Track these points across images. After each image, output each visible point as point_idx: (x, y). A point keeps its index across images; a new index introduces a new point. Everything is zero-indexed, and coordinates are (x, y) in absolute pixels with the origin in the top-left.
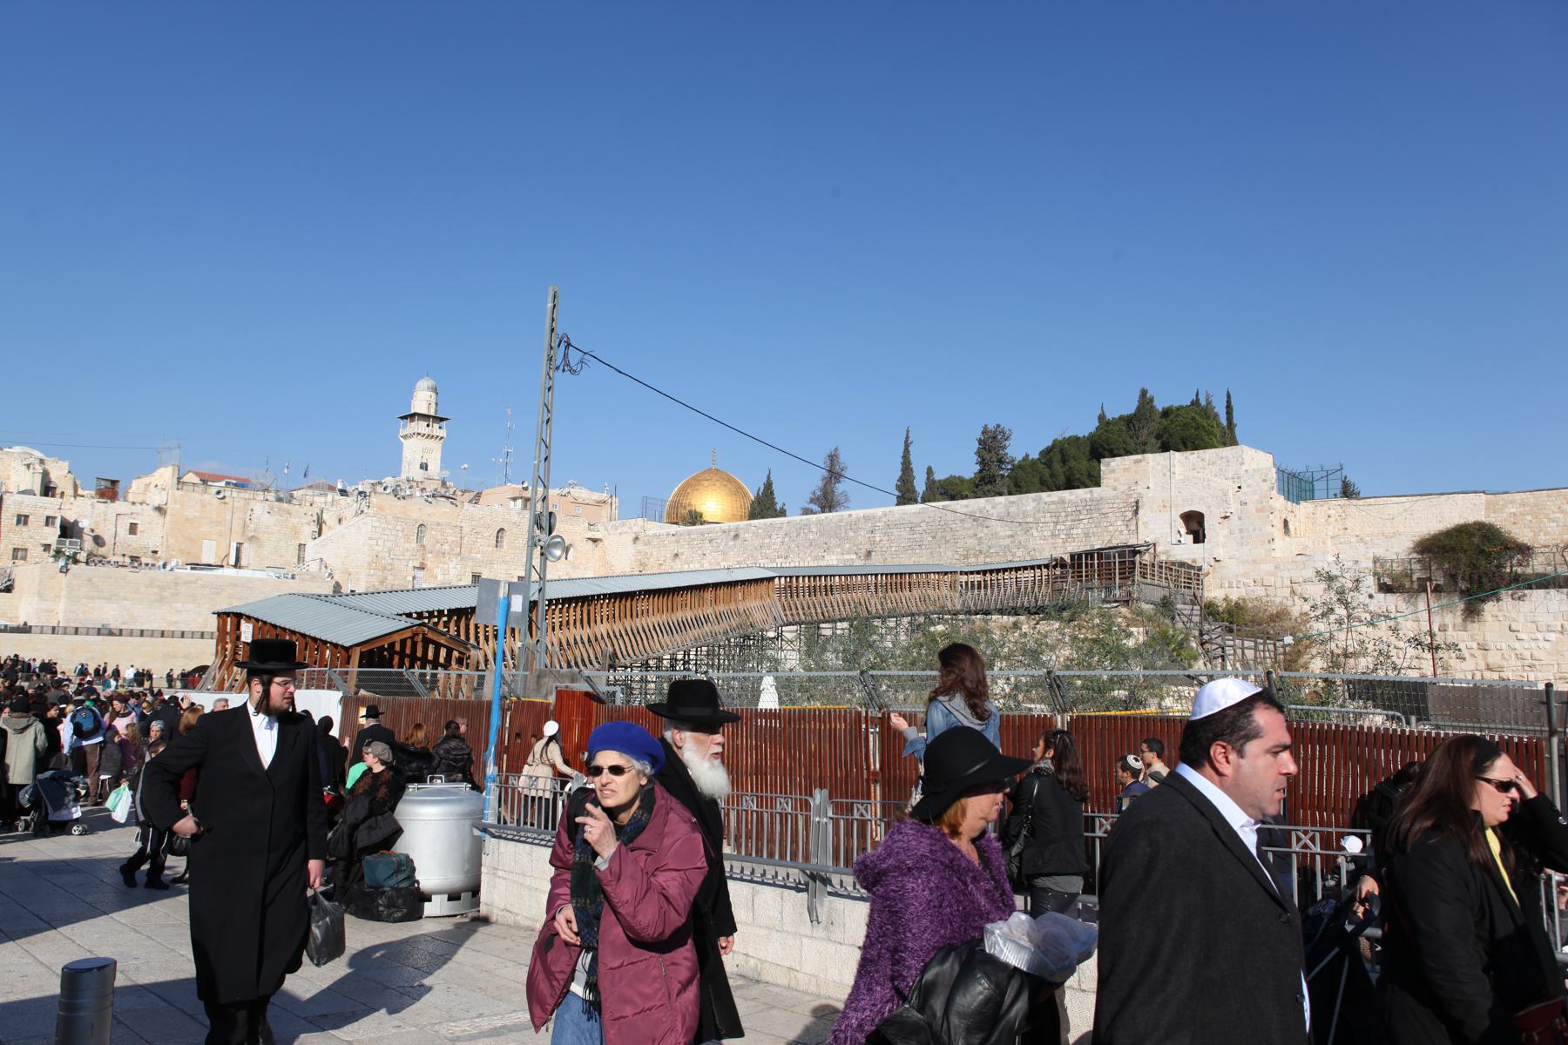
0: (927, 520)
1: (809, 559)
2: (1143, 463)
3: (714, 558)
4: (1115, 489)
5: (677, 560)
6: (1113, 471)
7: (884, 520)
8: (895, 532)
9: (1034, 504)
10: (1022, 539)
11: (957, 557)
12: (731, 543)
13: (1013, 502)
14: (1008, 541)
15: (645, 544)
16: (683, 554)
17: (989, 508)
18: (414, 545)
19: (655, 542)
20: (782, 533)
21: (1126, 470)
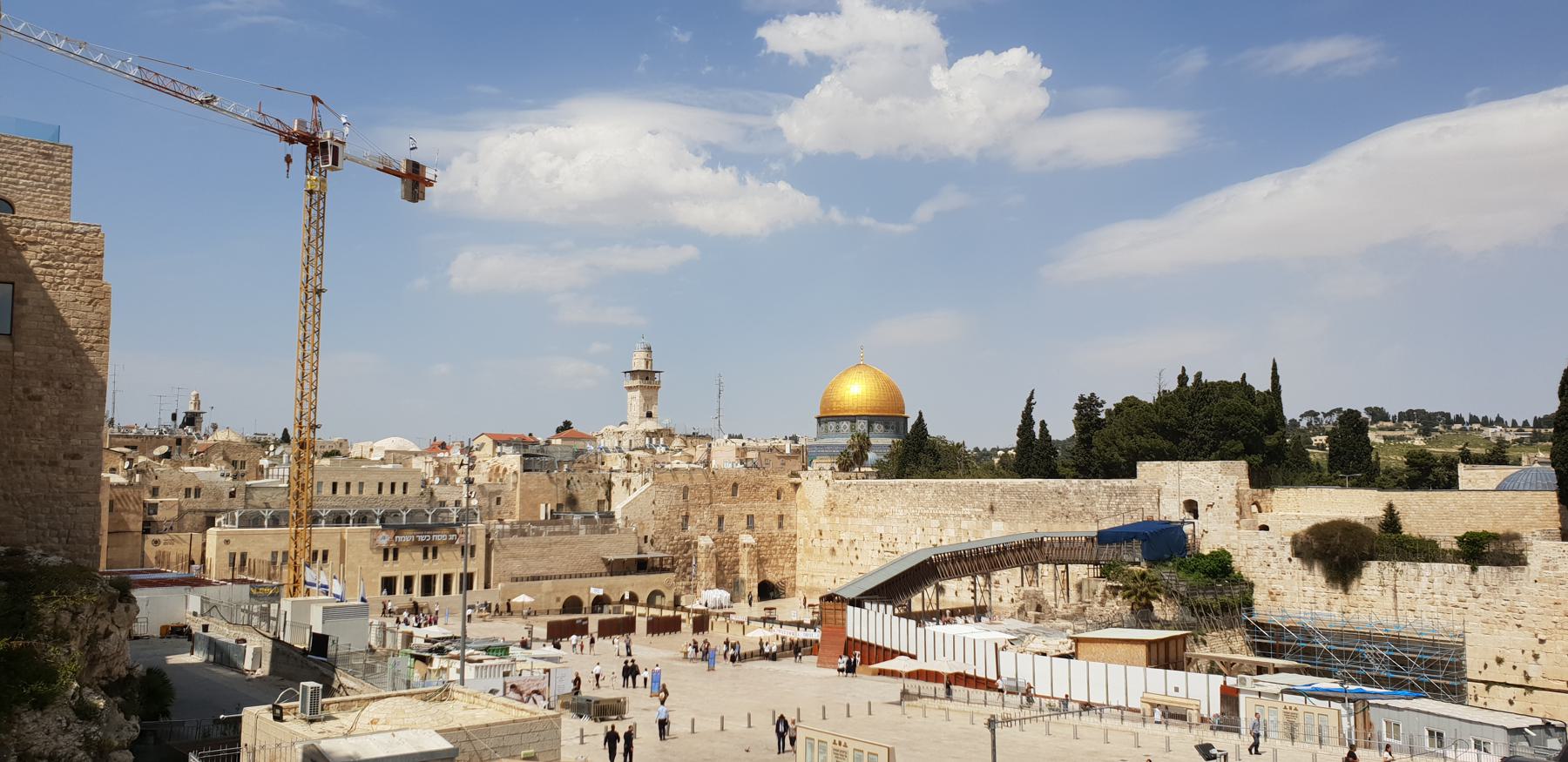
2: (1162, 467)
11: (1049, 516)
12: (897, 494)
14: (1080, 509)
15: (834, 489)
17: (1068, 486)
18: (681, 500)
20: (932, 491)
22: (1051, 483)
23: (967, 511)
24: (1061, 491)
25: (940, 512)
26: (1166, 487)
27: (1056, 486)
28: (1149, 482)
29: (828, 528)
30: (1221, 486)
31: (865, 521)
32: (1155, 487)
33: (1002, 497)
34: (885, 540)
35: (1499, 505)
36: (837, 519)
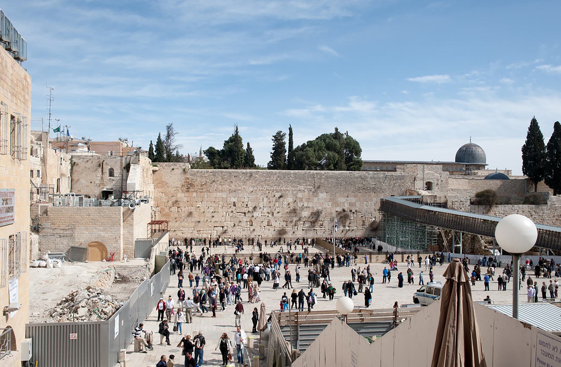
0: (343, 177)
1: (290, 187)
2: (416, 167)
3: (238, 183)
4: (408, 173)
5: (214, 183)
6: (408, 168)
7: (325, 175)
8: (330, 180)
9: (383, 175)
10: (379, 185)
13: (375, 174)
15: (192, 175)
16: (218, 181)
17: (367, 175)
19: (199, 174)
21: (412, 168)
22: (356, 173)
23: (302, 188)
24: (363, 177)
25: (282, 188)
26: (418, 175)
27: (360, 175)
28: (410, 173)
29: (185, 199)
30: (442, 176)
31: (219, 194)
32: (413, 176)
33: (326, 180)
34: (239, 205)
35: (506, 185)
36: (194, 194)
